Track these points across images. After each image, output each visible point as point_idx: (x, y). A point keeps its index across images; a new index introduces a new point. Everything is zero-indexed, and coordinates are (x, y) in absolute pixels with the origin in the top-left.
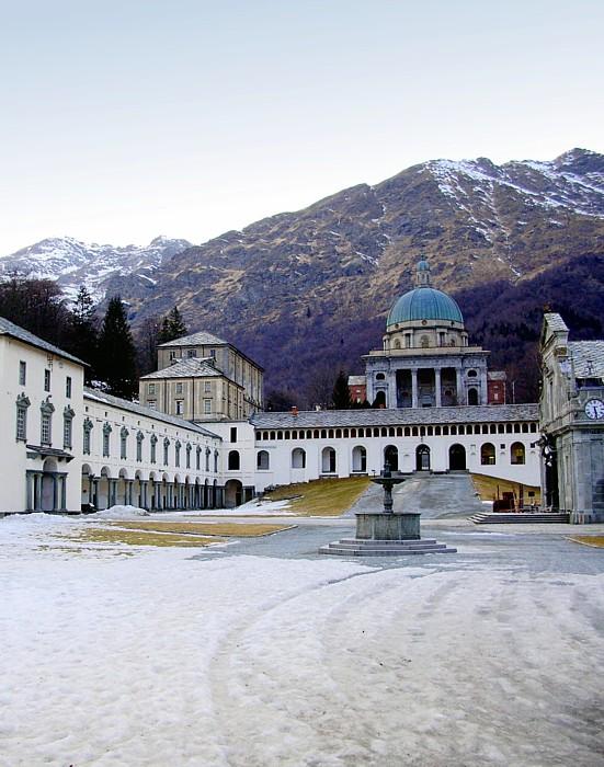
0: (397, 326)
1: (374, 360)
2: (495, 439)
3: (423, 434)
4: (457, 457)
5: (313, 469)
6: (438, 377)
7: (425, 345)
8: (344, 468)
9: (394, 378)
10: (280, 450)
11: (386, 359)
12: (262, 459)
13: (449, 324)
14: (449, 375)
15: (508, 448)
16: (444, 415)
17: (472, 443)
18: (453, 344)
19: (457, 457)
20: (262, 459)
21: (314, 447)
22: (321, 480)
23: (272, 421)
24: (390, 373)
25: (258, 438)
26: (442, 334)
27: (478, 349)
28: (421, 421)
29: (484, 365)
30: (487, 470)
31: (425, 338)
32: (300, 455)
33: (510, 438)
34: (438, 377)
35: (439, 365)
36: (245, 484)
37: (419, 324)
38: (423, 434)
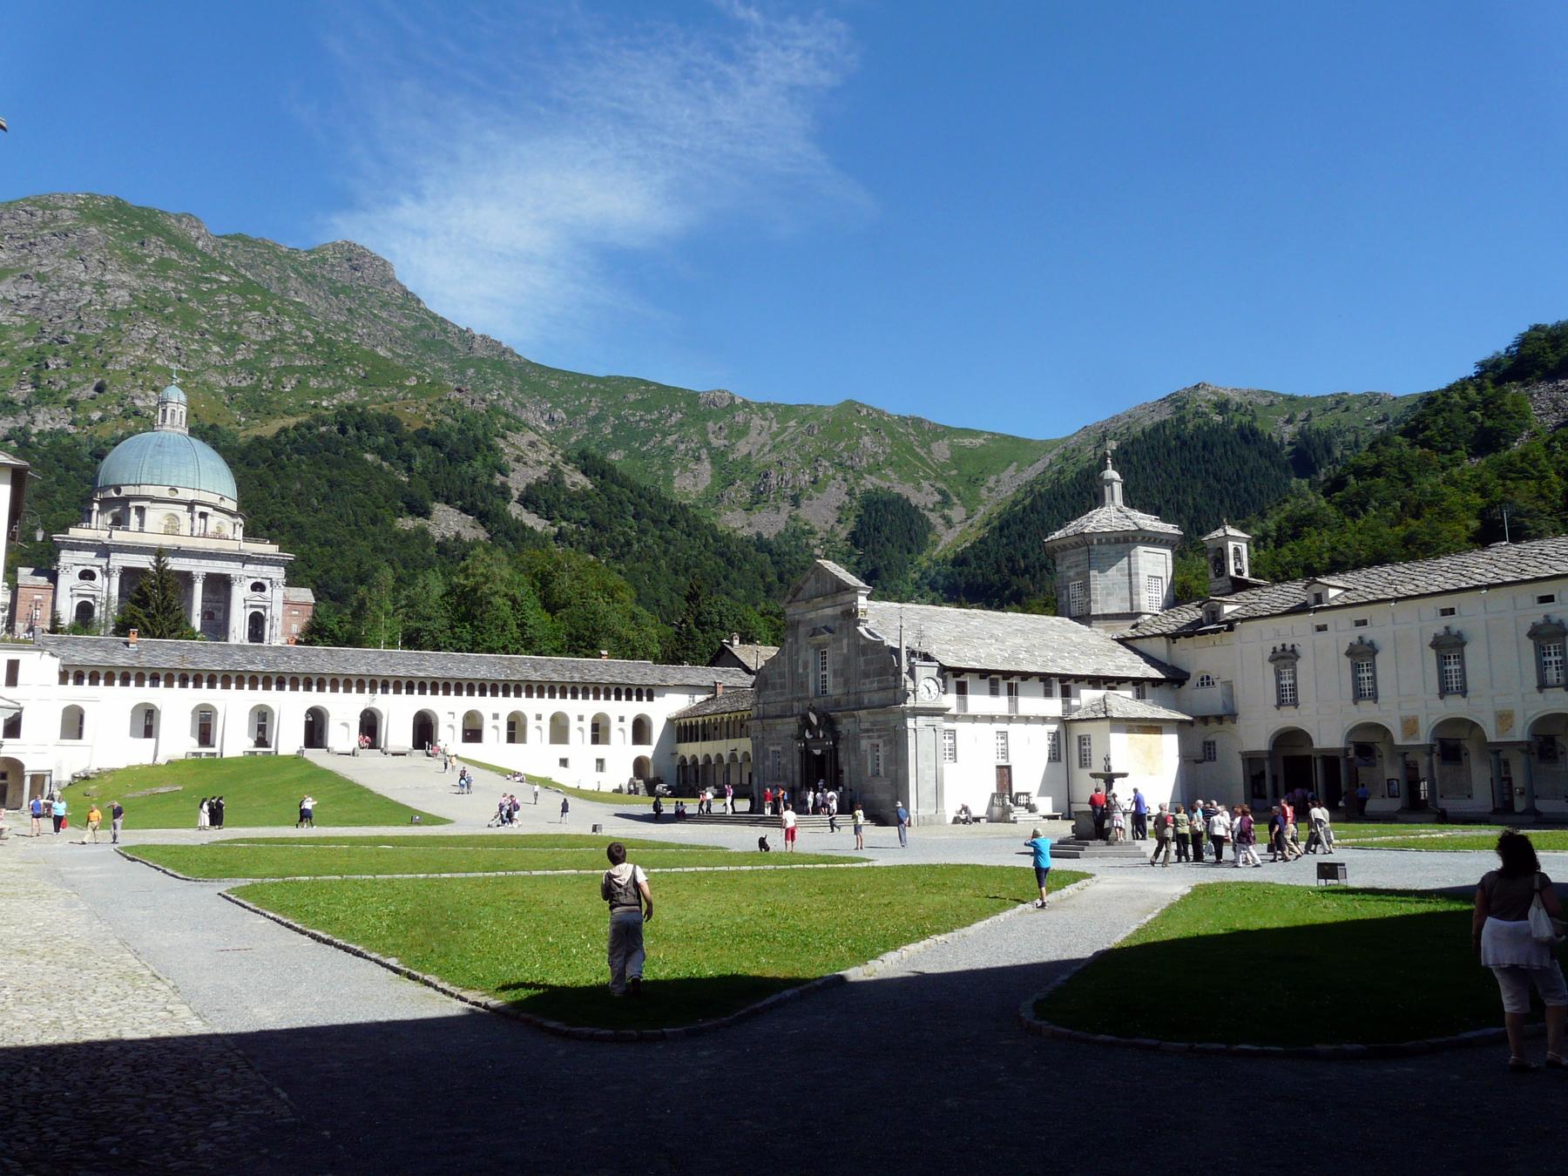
0: (118, 491)
1: (77, 546)
2: (487, 705)
3: (373, 691)
4: (424, 731)
5: (176, 740)
6: (198, 588)
7: (172, 529)
8: (235, 740)
9: (116, 581)
10: (109, 706)
11: (104, 550)
12: (74, 723)
13: (215, 499)
14: (219, 586)
15: (546, 724)
16: (405, 662)
17: (449, 710)
18: (218, 536)
19: (424, 731)
20: (74, 723)
21: (177, 706)
22: (194, 764)
23: (87, 653)
24: (107, 573)
25: (63, 678)
26: (203, 515)
27: (270, 549)
28: (373, 672)
29: (278, 574)
30: (471, 750)
31: (174, 517)
32: (147, 722)
33: (505, 705)
34: (198, 588)
35: (200, 568)
36: (31, 765)
37: (164, 493)
38: (373, 691)
